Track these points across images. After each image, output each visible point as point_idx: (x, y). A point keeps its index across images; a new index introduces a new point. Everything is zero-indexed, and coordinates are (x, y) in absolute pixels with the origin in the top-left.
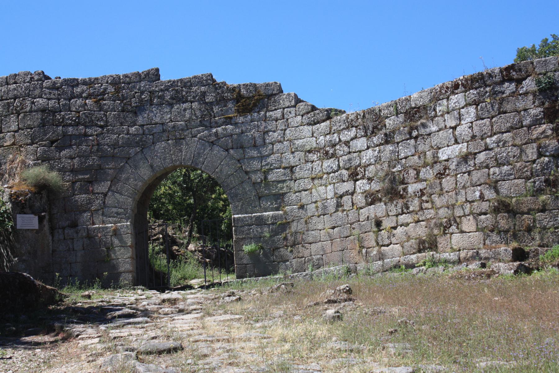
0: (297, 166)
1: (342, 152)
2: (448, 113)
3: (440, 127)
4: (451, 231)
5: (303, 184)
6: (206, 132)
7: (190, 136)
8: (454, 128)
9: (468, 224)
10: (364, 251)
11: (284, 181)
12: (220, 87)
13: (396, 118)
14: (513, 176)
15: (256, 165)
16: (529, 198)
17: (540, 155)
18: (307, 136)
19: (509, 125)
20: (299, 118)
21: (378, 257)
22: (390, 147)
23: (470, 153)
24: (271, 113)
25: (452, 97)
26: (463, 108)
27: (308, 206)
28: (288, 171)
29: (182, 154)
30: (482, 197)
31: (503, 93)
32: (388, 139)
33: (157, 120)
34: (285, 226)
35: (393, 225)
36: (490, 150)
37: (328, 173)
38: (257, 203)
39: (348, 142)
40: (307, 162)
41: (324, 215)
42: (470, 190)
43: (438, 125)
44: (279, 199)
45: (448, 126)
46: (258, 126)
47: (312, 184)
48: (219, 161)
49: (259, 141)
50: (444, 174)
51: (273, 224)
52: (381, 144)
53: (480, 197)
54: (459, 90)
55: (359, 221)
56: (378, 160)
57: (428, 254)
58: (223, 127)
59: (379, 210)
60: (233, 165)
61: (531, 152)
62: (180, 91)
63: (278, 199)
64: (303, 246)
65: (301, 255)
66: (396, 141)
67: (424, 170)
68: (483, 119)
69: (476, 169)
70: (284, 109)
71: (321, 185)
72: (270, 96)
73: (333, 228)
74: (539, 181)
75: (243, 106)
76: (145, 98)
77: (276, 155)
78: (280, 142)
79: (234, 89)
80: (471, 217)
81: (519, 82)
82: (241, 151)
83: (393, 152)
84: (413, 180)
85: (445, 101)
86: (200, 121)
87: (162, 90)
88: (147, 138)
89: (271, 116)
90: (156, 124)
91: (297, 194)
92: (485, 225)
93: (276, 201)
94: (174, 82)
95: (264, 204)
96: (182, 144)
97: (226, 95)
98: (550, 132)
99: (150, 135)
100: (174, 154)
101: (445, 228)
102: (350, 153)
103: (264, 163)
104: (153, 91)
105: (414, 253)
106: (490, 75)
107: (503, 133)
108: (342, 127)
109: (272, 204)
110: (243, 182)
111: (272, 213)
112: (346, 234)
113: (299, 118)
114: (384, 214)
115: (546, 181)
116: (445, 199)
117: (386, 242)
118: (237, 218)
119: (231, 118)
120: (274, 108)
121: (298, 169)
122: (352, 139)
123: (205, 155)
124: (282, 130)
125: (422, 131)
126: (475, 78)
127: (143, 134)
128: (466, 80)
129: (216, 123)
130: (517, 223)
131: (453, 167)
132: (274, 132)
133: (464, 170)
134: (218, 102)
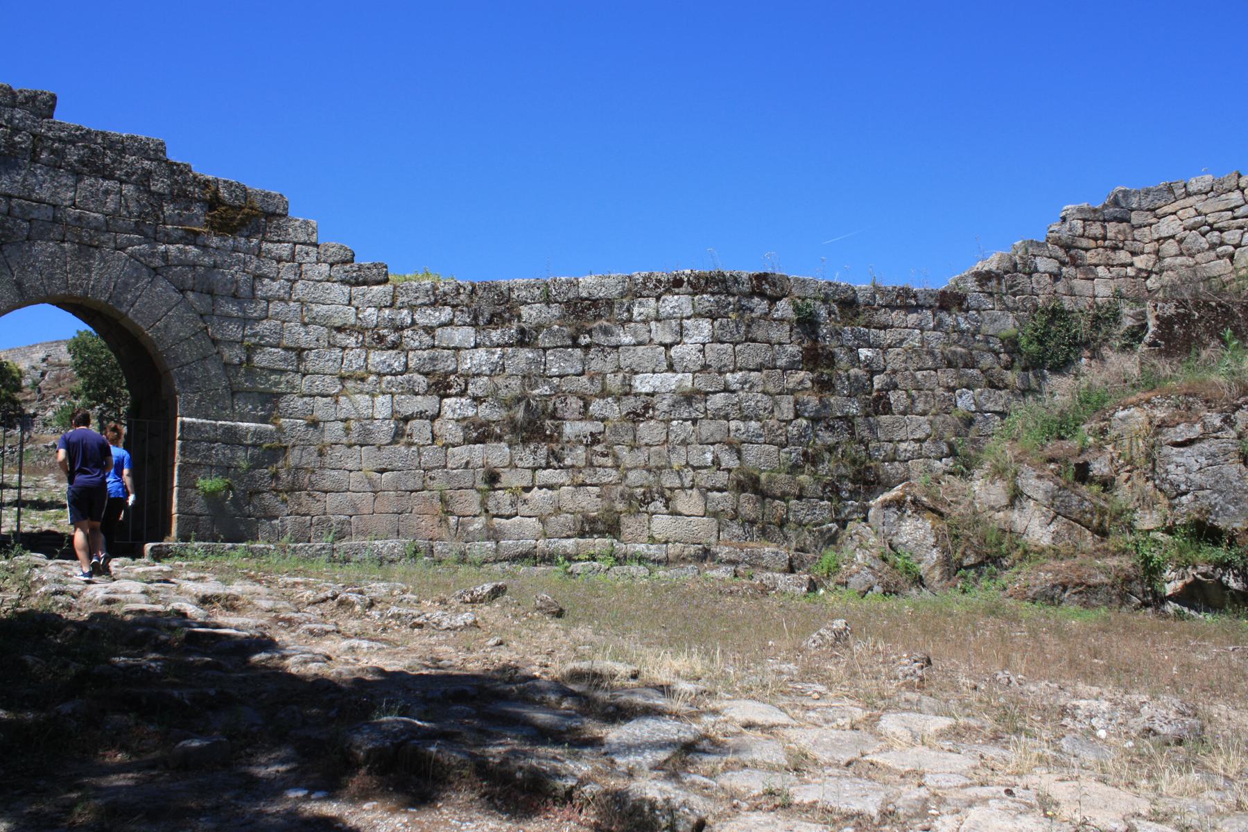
0: (311, 349)
1: (417, 344)
2: (658, 320)
3: (640, 339)
4: (651, 508)
5: (319, 383)
6: (145, 246)
7: (113, 245)
8: (668, 347)
9: (689, 503)
10: (452, 520)
11: (282, 372)
12: (181, 172)
13: (545, 308)
14: (762, 439)
15: (233, 331)
16: (783, 475)
17: (797, 416)
18: (335, 302)
19: (759, 360)
20: (325, 268)
21: (485, 535)
22: (527, 353)
23: (698, 392)
24: (270, 245)
25: (669, 297)
26: (688, 318)
27: (328, 425)
28: (293, 355)
29: (90, 277)
30: (716, 462)
31: (752, 311)
32: (524, 339)
33: (45, 194)
34: (278, 452)
35: (525, 484)
36: (734, 392)
37: (379, 375)
38: (228, 402)
39: (432, 328)
40: (332, 346)
41: (361, 446)
42: (695, 449)
43: (635, 334)
44: (270, 401)
45: (657, 340)
46: (245, 263)
47: (340, 387)
48: (165, 309)
49: (244, 290)
50: (643, 415)
51: (254, 446)
52: (511, 345)
53: (713, 462)
54: (682, 289)
55: (445, 467)
56: (498, 370)
57: (599, 544)
58: (181, 246)
59: (497, 454)
60: (191, 322)
61: (786, 407)
62: (98, 156)
63: (267, 401)
64: (309, 495)
65: (304, 510)
66: (541, 344)
67: (602, 402)
68: (722, 342)
69: (706, 417)
70: (295, 244)
71: (361, 392)
72: (271, 215)
73: (382, 471)
74: (793, 453)
75: (222, 218)
76: (20, 143)
77: (273, 322)
78: (282, 300)
79: (206, 184)
80: (695, 492)
81: (773, 300)
82: (210, 300)
83: (530, 362)
84: (576, 415)
85: (652, 301)
86: (136, 223)
87: (60, 140)
88: (15, 224)
89: (269, 251)
90: (41, 201)
91: (306, 399)
92: (720, 507)
93: (264, 405)
94: (89, 132)
95: (239, 406)
96: (92, 256)
97: (191, 189)
98: (809, 384)
99: (25, 221)
100: (73, 271)
101: (641, 502)
102: (433, 347)
103: (248, 331)
104: (42, 135)
105: (568, 537)
106: (736, 280)
107: (750, 370)
108: (419, 301)
109: (255, 409)
110: (205, 358)
111: (254, 424)
112: (411, 486)
113: (325, 268)
114: (507, 462)
115: (805, 454)
116: (641, 456)
117: (508, 510)
118: (189, 423)
119: (197, 234)
120: (276, 238)
121: (312, 355)
122: (442, 325)
123: (137, 289)
124: (288, 280)
125: (602, 339)
126: (713, 278)
127: (9, 214)
128: (698, 277)
129: (167, 234)
130: (767, 511)
131: (663, 405)
132: (273, 279)
133: (685, 415)
134: (174, 198)
